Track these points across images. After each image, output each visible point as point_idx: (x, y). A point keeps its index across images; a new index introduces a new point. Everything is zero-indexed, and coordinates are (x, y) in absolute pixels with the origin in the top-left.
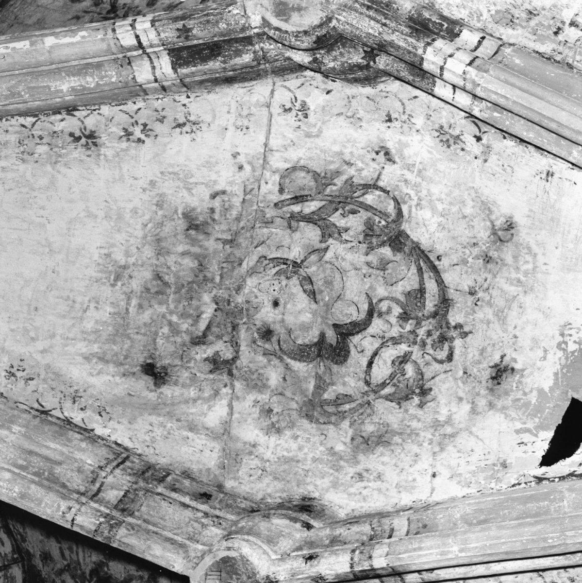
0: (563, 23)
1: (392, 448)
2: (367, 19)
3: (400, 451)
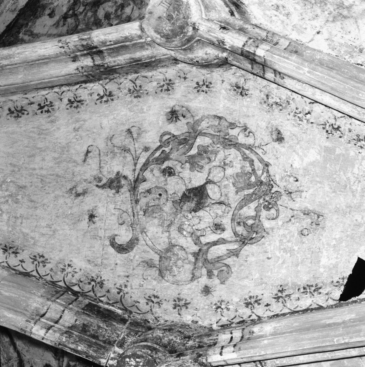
1: (307, 3)
3: (309, 7)
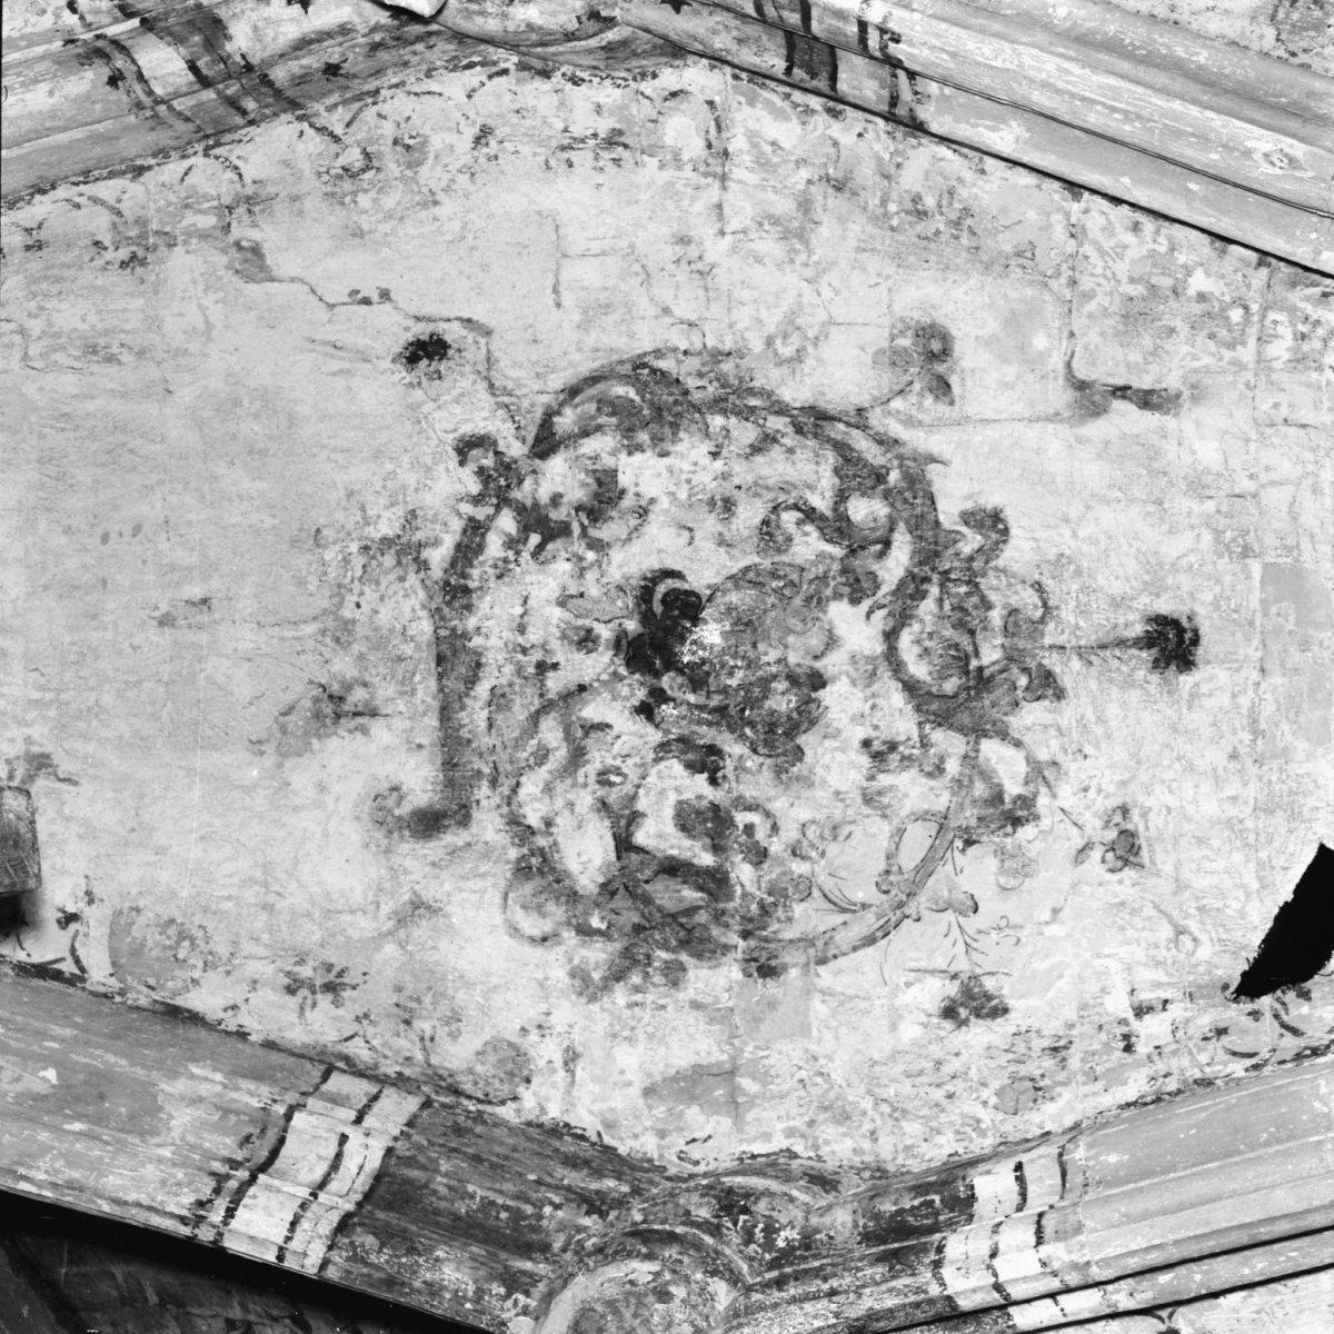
0: (1123, 1022)
2: (793, 1308)
